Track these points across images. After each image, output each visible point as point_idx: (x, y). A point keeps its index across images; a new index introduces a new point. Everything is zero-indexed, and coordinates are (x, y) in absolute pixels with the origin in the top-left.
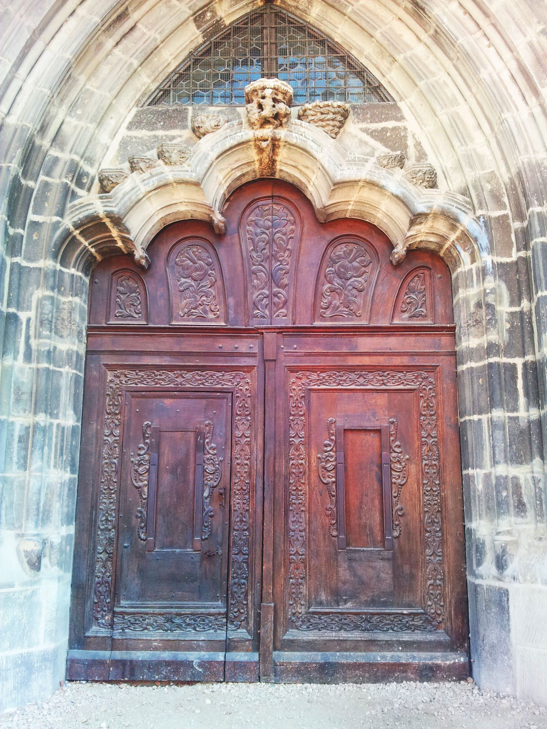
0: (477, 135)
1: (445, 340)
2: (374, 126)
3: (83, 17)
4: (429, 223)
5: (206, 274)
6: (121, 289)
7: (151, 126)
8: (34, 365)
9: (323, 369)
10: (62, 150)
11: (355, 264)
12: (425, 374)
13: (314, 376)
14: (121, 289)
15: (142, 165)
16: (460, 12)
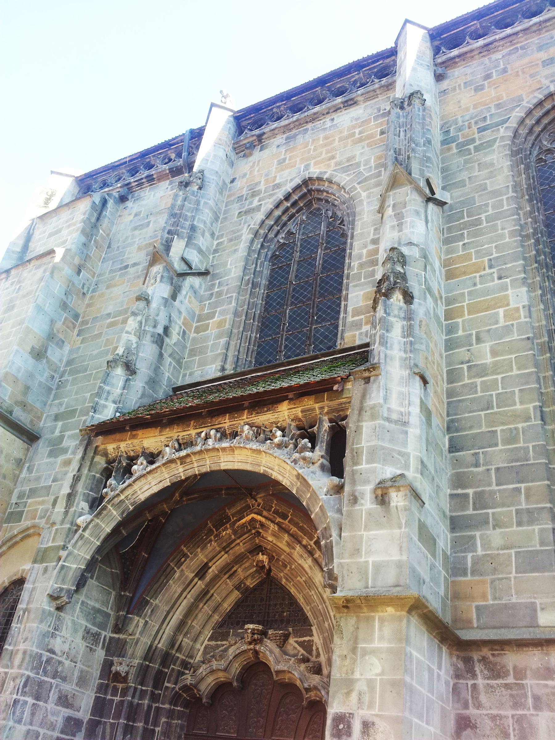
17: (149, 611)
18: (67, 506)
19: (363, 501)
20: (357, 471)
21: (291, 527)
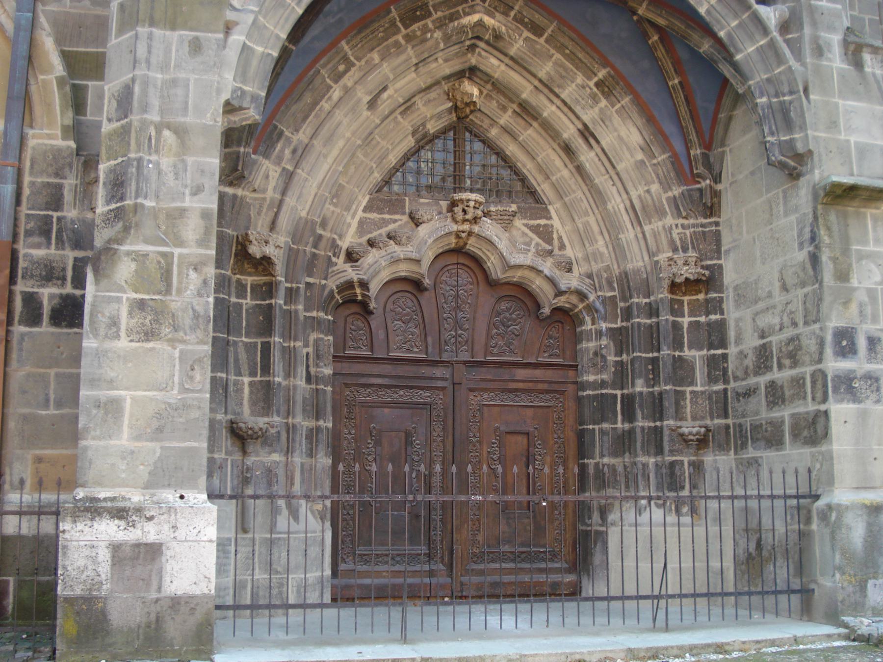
0: (599, 238)
1: (571, 373)
2: (532, 222)
3: (349, 139)
4: (567, 296)
6: (353, 327)
7: (380, 211)
8: (314, 386)
9: (493, 390)
10: (324, 230)
11: (514, 316)
12: (558, 396)
13: (486, 395)
14: (353, 327)
15: (381, 245)
16: (596, 159)
17: (287, 152)
19: (830, 56)
20: (816, 7)
21: (552, 51)
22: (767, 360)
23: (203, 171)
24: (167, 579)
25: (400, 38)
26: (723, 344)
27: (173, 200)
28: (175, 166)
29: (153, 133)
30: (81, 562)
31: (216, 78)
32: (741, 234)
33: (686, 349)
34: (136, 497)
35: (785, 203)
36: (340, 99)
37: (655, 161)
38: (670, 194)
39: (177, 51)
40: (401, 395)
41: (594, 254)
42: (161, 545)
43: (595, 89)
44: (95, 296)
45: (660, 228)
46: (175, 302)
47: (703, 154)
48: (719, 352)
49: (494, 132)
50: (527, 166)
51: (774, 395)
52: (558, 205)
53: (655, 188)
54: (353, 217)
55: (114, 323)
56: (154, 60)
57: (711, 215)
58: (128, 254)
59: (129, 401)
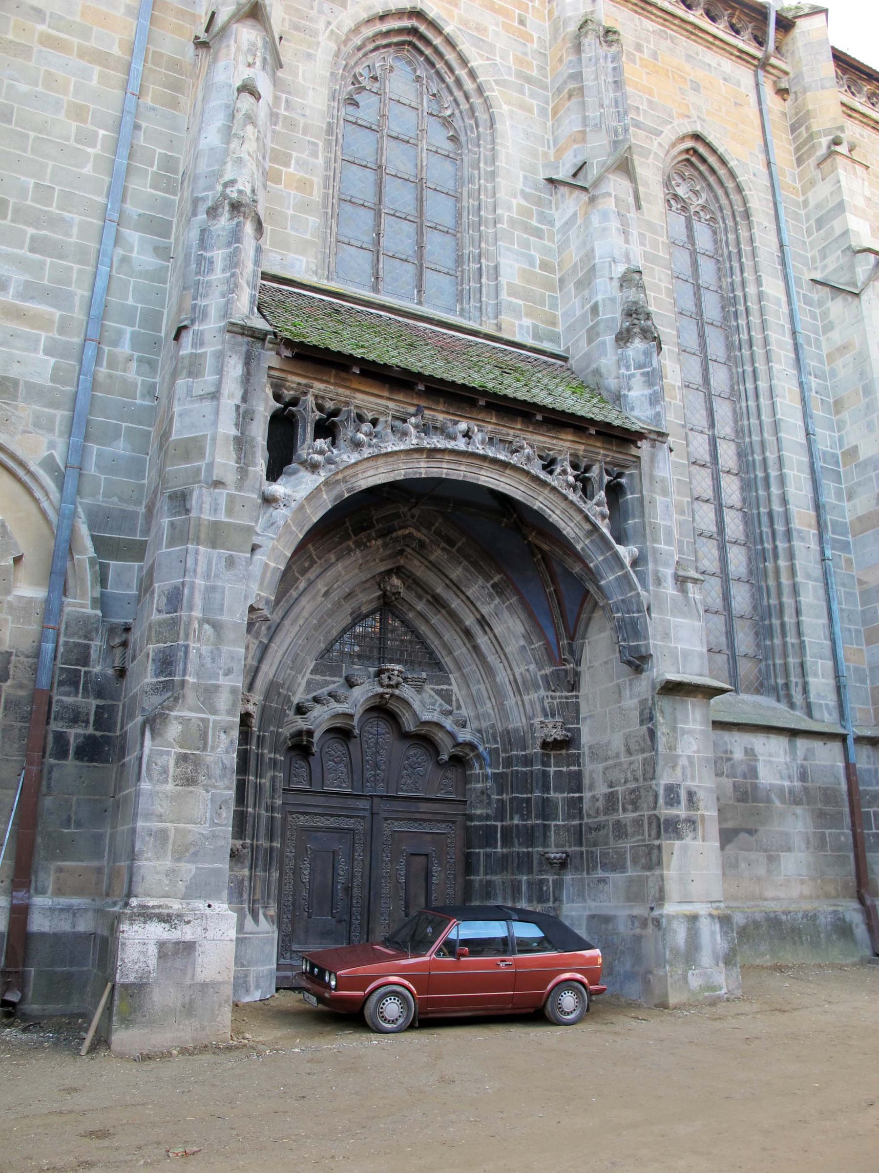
0: (488, 702)
1: (461, 807)
5: (342, 760)
7: (323, 674)
12: (451, 825)
13: (396, 823)
16: (489, 642)
17: (263, 628)
18: (239, 458)
19: (666, 585)
22: (614, 804)
23: (233, 658)
24: (198, 969)
25: (351, 543)
26: (579, 789)
27: (210, 678)
28: (212, 653)
29: (197, 626)
30: (135, 956)
31: (244, 587)
32: (595, 707)
33: (552, 792)
34: (176, 906)
35: (631, 690)
36: (305, 589)
37: (533, 647)
38: (543, 672)
39: (217, 565)
40: (331, 822)
41: (483, 715)
42: (195, 943)
43: (491, 589)
44: (151, 750)
45: (536, 699)
46: (209, 757)
47: (569, 643)
48: (577, 795)
49: (411, 615)
50: (434, 643)
51: (619, 831)
52: (457, 675)
53: (532, 667)
54: (303, 678)
55: (165, 771)
56: (199, 570)
57: (572, 691)
58: (176, 718)
59: (173, 831)
